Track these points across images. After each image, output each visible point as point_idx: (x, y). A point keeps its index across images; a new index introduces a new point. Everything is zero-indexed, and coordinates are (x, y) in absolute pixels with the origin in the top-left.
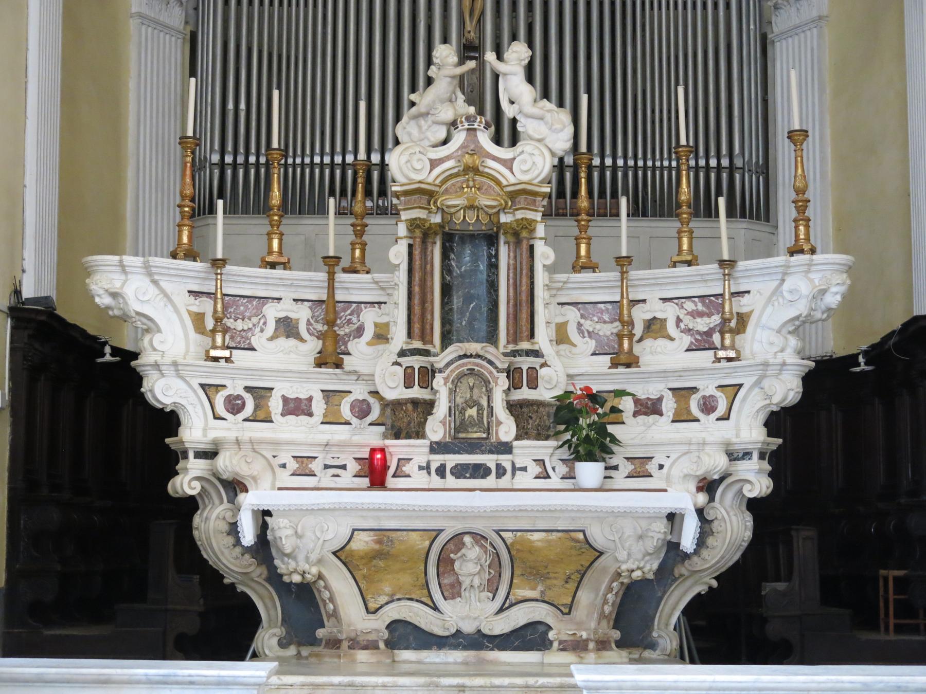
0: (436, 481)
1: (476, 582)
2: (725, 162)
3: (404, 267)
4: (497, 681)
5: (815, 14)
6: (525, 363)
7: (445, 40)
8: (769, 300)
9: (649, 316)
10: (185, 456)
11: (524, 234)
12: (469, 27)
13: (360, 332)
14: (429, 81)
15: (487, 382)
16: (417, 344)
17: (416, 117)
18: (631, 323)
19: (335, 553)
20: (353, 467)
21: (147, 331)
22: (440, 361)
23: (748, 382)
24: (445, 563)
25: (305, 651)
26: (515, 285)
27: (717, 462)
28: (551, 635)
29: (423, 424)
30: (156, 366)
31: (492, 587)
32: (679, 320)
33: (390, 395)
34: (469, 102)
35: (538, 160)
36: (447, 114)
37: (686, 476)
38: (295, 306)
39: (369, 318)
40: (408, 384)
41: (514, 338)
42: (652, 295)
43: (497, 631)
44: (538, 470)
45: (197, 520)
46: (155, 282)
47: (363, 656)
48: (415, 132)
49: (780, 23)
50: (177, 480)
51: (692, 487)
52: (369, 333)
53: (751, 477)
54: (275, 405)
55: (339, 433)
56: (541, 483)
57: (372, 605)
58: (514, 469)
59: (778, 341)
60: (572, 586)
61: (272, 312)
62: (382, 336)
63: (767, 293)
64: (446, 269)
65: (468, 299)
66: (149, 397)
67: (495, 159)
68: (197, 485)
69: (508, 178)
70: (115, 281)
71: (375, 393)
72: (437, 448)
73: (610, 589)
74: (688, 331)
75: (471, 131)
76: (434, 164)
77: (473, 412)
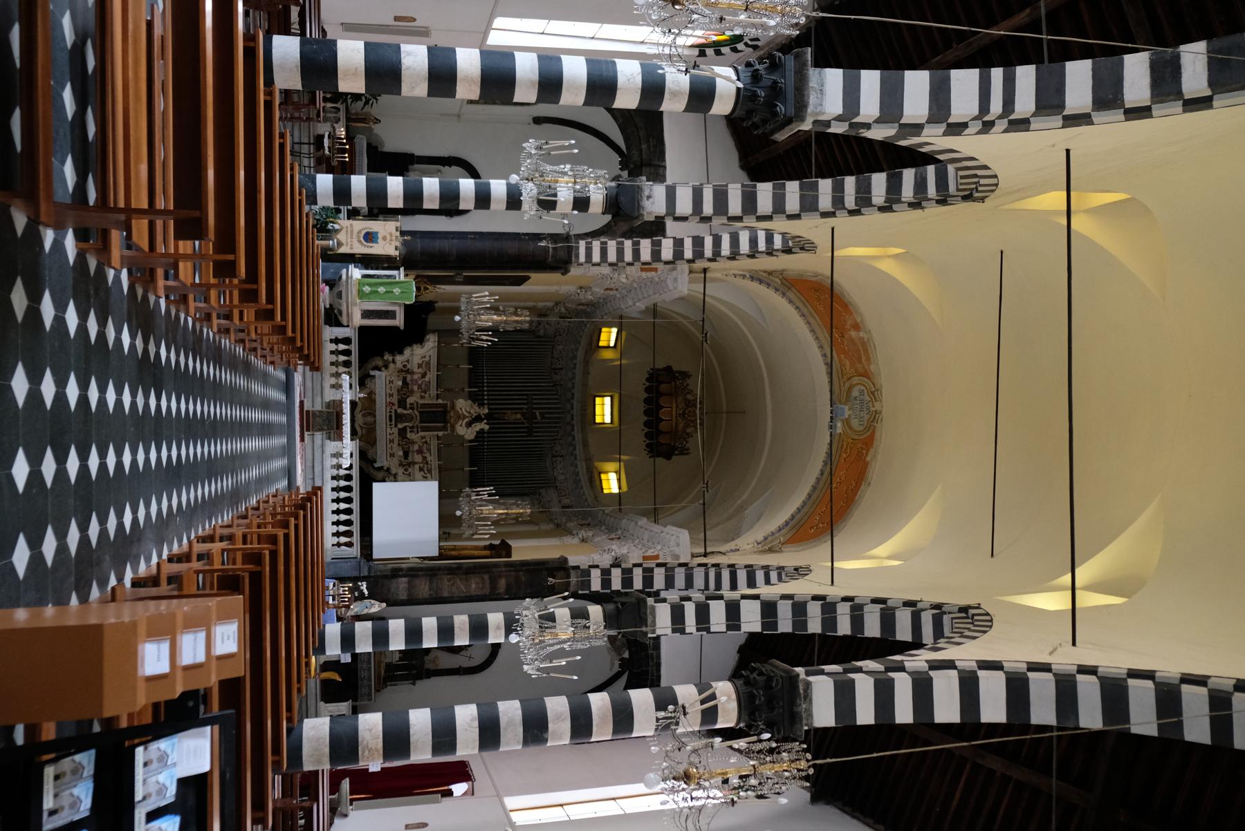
10: (393, 356)
19: (372, 391)
20: (391, 393)
22: (416, 411)
24: (370, 414)
30: (413, 350)
31: (365, 424)
33: (408, 400)
34: (476, 416)
36: (472, 412)
37: (390, 465)
40: (411, 404)
41: (421, 427)
45: (379, 358)
51: (388, 466)
56: (388, 434)
62: (422, 397)
71: (408, 396)
72: (396, 411)
75: (467, 417)
76: (461, 409)
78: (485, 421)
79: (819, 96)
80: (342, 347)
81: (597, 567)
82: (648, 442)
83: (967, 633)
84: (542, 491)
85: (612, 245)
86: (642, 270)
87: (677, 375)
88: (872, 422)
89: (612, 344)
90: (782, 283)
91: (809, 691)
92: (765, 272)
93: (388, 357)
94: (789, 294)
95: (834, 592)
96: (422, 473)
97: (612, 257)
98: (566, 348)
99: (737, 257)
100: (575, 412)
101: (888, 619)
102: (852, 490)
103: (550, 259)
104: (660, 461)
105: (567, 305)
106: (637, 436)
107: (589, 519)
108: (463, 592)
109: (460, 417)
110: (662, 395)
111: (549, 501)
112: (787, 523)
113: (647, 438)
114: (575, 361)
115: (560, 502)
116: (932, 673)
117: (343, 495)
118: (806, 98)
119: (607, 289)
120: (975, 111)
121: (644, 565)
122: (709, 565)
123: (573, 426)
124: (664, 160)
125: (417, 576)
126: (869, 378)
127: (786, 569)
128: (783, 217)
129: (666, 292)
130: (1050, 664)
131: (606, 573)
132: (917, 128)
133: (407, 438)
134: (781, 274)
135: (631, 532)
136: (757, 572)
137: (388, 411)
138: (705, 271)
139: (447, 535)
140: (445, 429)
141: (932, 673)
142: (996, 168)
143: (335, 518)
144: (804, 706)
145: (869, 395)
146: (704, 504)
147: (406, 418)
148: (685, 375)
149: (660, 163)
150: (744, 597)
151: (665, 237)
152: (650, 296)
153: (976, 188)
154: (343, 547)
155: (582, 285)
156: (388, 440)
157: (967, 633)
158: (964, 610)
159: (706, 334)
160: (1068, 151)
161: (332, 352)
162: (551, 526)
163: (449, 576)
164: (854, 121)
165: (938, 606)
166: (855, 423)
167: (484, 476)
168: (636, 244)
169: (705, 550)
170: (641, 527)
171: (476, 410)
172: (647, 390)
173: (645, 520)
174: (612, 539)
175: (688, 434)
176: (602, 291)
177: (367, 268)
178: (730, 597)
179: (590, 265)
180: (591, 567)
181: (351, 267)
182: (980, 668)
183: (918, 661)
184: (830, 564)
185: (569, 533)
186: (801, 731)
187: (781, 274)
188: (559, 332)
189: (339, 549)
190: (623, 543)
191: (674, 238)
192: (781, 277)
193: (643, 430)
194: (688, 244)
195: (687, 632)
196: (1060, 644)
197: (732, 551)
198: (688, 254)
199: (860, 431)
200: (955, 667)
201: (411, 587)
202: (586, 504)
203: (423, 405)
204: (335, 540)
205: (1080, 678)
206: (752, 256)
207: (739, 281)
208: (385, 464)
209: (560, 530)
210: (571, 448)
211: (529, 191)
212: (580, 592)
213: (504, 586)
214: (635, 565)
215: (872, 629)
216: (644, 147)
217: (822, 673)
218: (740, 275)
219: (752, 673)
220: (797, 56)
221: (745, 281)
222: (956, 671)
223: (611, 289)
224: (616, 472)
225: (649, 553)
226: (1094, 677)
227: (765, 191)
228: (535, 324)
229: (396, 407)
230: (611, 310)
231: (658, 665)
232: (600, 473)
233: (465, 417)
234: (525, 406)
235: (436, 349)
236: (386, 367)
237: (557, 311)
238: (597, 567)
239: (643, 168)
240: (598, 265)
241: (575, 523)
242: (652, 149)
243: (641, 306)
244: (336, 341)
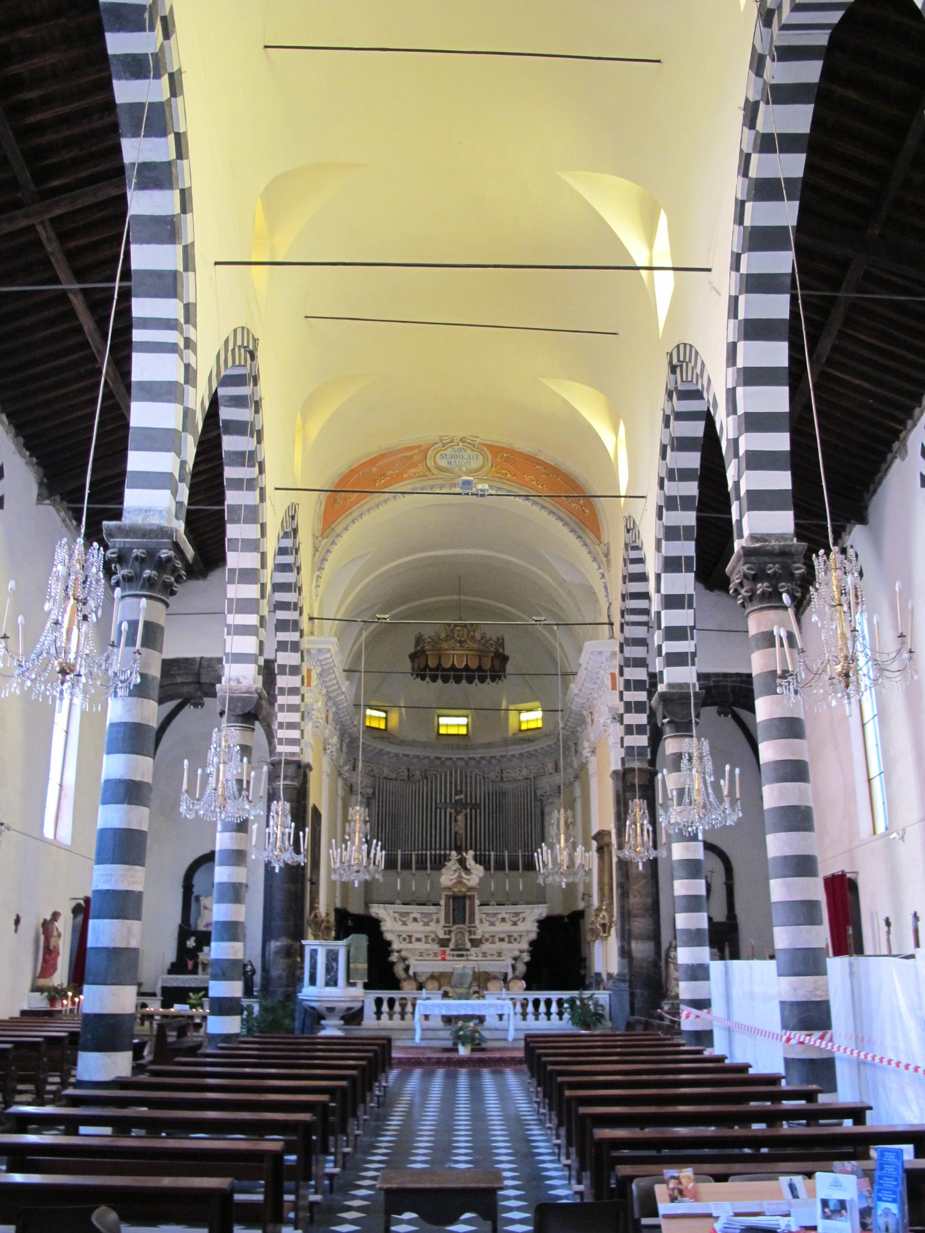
0: (452, 958)
6: (473, 929)
10: (392, 951)
14: (450, 860)
16: (447, 925)
20: (432, 954)
22: (453, 929)
27: (517, 953)
30: (388, 931)
36: (454, 868)
39: (434, 917)
40: (445, 934)
49: (547, 810)
52: (435, 920)
54: (413, 939)
55: (428, 946)
61: (412, 916)
62: (438, 921)
64: (454, 905)
71: (437, 936)
72: (453, 950)
75: (460, 873)
76: (451, 880)
78: (464, 854)
79: (151, 513)
80: (385, 1008)
81: (622, 739)
82: (489, 680)
83: (698, 370)
84: (539, 793)
85: (282, 717)
86: (309, 685)
87: (419, 648)
88: (474, 446)
89: (383, 715)
90: (327, 537)
91: (758, 536)
92: (314, 555)
93: (394, 958)
94: (338, 529)
95: (654, 498)
96: (519, 923)
97: (295, 717)
99: (299, 585)
100: (454, 756)
101: (682, 444)
102: (545, 469)
103: (296, 784)
104: (509, 668)
105: (341, 764)
106: (482, 691)
107: (570, 743)
109: (460, 882)
110: (440, 665)
111: (550, 786)
112: (579, 537)
114: (401, 756)
115: (551, 774)
116: (740, 411)
117: (542, 1008)
118: (153, 527)
119: (327, 722)
120: (176, 356)
121: (622, 689)
122: (623, 621)
123: (470, 759)
124: (194, 659)
125: (629, 930)
126: (428, 449)
127: (628, 542)
128: (263, 541)
129: (333, 661)
130: (730, 297)
131: (629, 730)
132: (188, 414)
134: (317, 538)
135: (585, 701)
136: (630, 571)
138: (311, 619)
139: (586, 897)
140: (472, 898)
141: (740, 411)
142: (228, 332)
144: (773, 543)
145: (446, 449)
146: (558, 625)
147: (461, 939)
148: (419, 640)
149: (198, 664)
150: (658, 590)
151: (275, 661)
152: (336, 678)
153: (245, 347)
155: (321, 749)
157: (698, 370)
158: (673, 369)
159: (379, 619)
160: (216, 263)
161: (391, 1018)
162: (577, 784)
164: (177, 477)
165: (670, 394)
166: (475, 464)
168: (282, 691)
169: (605, 624)
170: (580, 690)
171: (452, 865)
172: (434, 679)
173: (572, 686)
174: (592, 720)
175: (482, 638)
177: (301, 980)
178: (658, 605)
179: (302, 740)
180: (622, 746)
181: (301, 996)
182: (734, 364)
183: (727, 426)
184: (622, 499)
185: (584, 766)
186: (799, 545)
187: (317, 538)
190: (597, 710)
191: (277, 651)
192: (320, 538)
194: (283, 636)
195: (694, 651)
196: (710, 283)
197: (607, 596)
198: (293, 636)
199: (484, 463)
200: (734, 389)
201: (642, 938)
202: (553, 746)
203: (447, 920)
205: (743, 270)
206: (299, 569)
207: (322, 582)
208: (510, 962)
209: (581, 774)
210: (494, 761)
211: (233, 811)
212: (649, 757)
214: (621, 699)
215: (692, 460)
216: (179, 680)
217: (739, 522)
218: (317, 582)
219: (740, 594)
220: (111, 535)
221: (323, 576)
222: (737, 388)
223: (327, 717)
224: (520, 713)
225: (609, 683)
226: (742, 256)
227: (235, 560)
229: (448, 950)
230: (348, 717)
231: (726, 675)
232: (521, 731)
233: (460, 877)
234: (448, 810)
235: (387, 905)
237: (347, 775)
238: (622, 739)
239: (202, 681)
240: (302, 731)
241: (574, 758)
242: (182, 672)
243: (345, 686)
244: (379, 1013)
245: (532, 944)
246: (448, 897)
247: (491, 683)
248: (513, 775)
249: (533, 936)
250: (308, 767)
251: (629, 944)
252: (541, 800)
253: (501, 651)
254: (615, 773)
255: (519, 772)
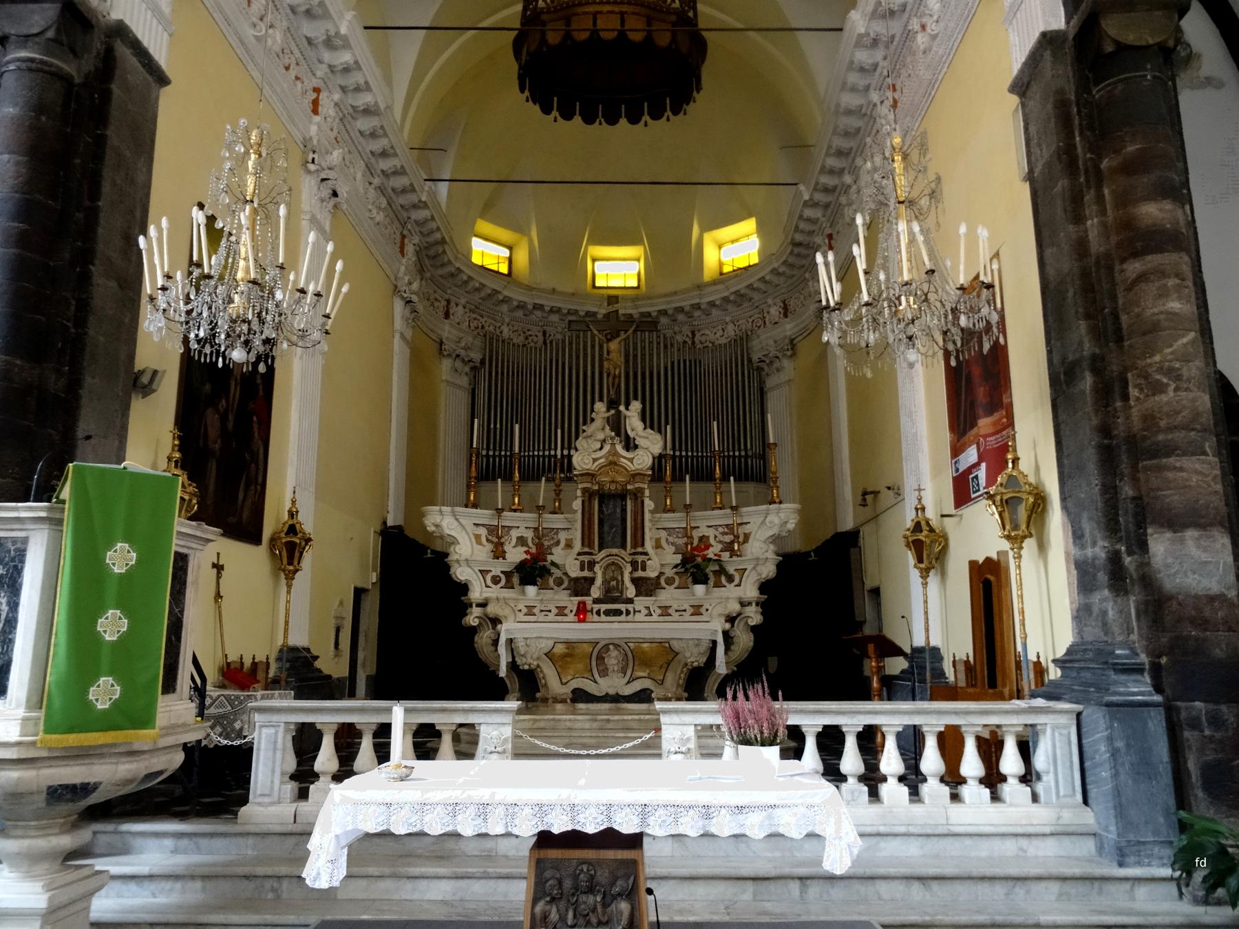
1: (616, 668)
2: (743, 453)
3: (580, 512)
4: (626, 717)
5: (787, 378)
6: (640, 558)
7: (601, 400)
8: (759, 527)
9: (701, 535)
10: (471, 606)
11: (639, 495)
12: (612, 392)
13: (558, 543)
14: (593, 420)
15: (621, 568)
16: (586, 550)
17: (585, 438)
18: (691, 537)
20: (555, 611)
21: (453, 543)
23: (749, 567)
24: (600, 659)
25: (530, 705)
26: (635, 520)
27: (734, 607)
28: (653, 695)
29: (589, 589)
30: (457, 561)
32: (716, 537)
33: (573, 575)
34: (612, 430)
35: (646, 458)
36: (601, 436)
38: (526, 531)
39: (563, 536)
40: (582, 569)
41: (635, 546)
42: (703, 525)
43: (626, 693)
44: (647, 612)
45: (476, 638)
46: (457, 520)
47: (559, 706)
48: (585, 445)
49: (770, 382)
50: (467, 618)
51: (723, 620)
53: (752, 615)
56: (648, 619)
57: (564, 681)
58: (635, 612)
59: (764, 547)
60: (663, 670)
61: (515, 534)
62: (569, 545)
63: (758, 524)
64: (601, 511)
65: (611, 527)
66: (453, 576)
67: (624, 458)
68: (477, 621)
69: (631, 467)
70: (438, 519)
71: (566, 574)
72: (596, 601)
73: (682, 672)
74: (720, 542)
75: (613, 444)
76: (595, 460)
77: (614, 583)
82: (669, 113)
84: (755, 358)
89: (505, 253)
93: (472, 619)
98: (507, 320)
108: (1193, 342)
109: (613, 463)
110: (568, 35)
111: (776, 342)
113: (663, 115)
115: (776, 323)
133: (658, 577)
137: (596, 618)
139: (869, 498)
140: (637, 496)
143: (933, 789)
147: (614, 579)
154: (1040, 760)
156: (662, 619)
163: (1134, 392)
167: (729, 457)
171: (597, 429)
176: (317, 119)
188: (477, 328)
189: (1048, 779)
193: (646, 125)
203: (587, 539)
204: (1012, 789)
210: (681, 317)
213: (1168, 205)
223: (315, 103)
228: (458, 364)
229: (589, 600)
232: (721, 274)
236: (495, 621)
245: (764, 587)
246: (589, 495)
247: (671, 117)
248: (712, 337)
249: (769, 570)
250: (120, 31)
251: (1141, 546)
252: (760, 369)
253: (691, 14)
254: (1048, 40)
255: (717, 332)
